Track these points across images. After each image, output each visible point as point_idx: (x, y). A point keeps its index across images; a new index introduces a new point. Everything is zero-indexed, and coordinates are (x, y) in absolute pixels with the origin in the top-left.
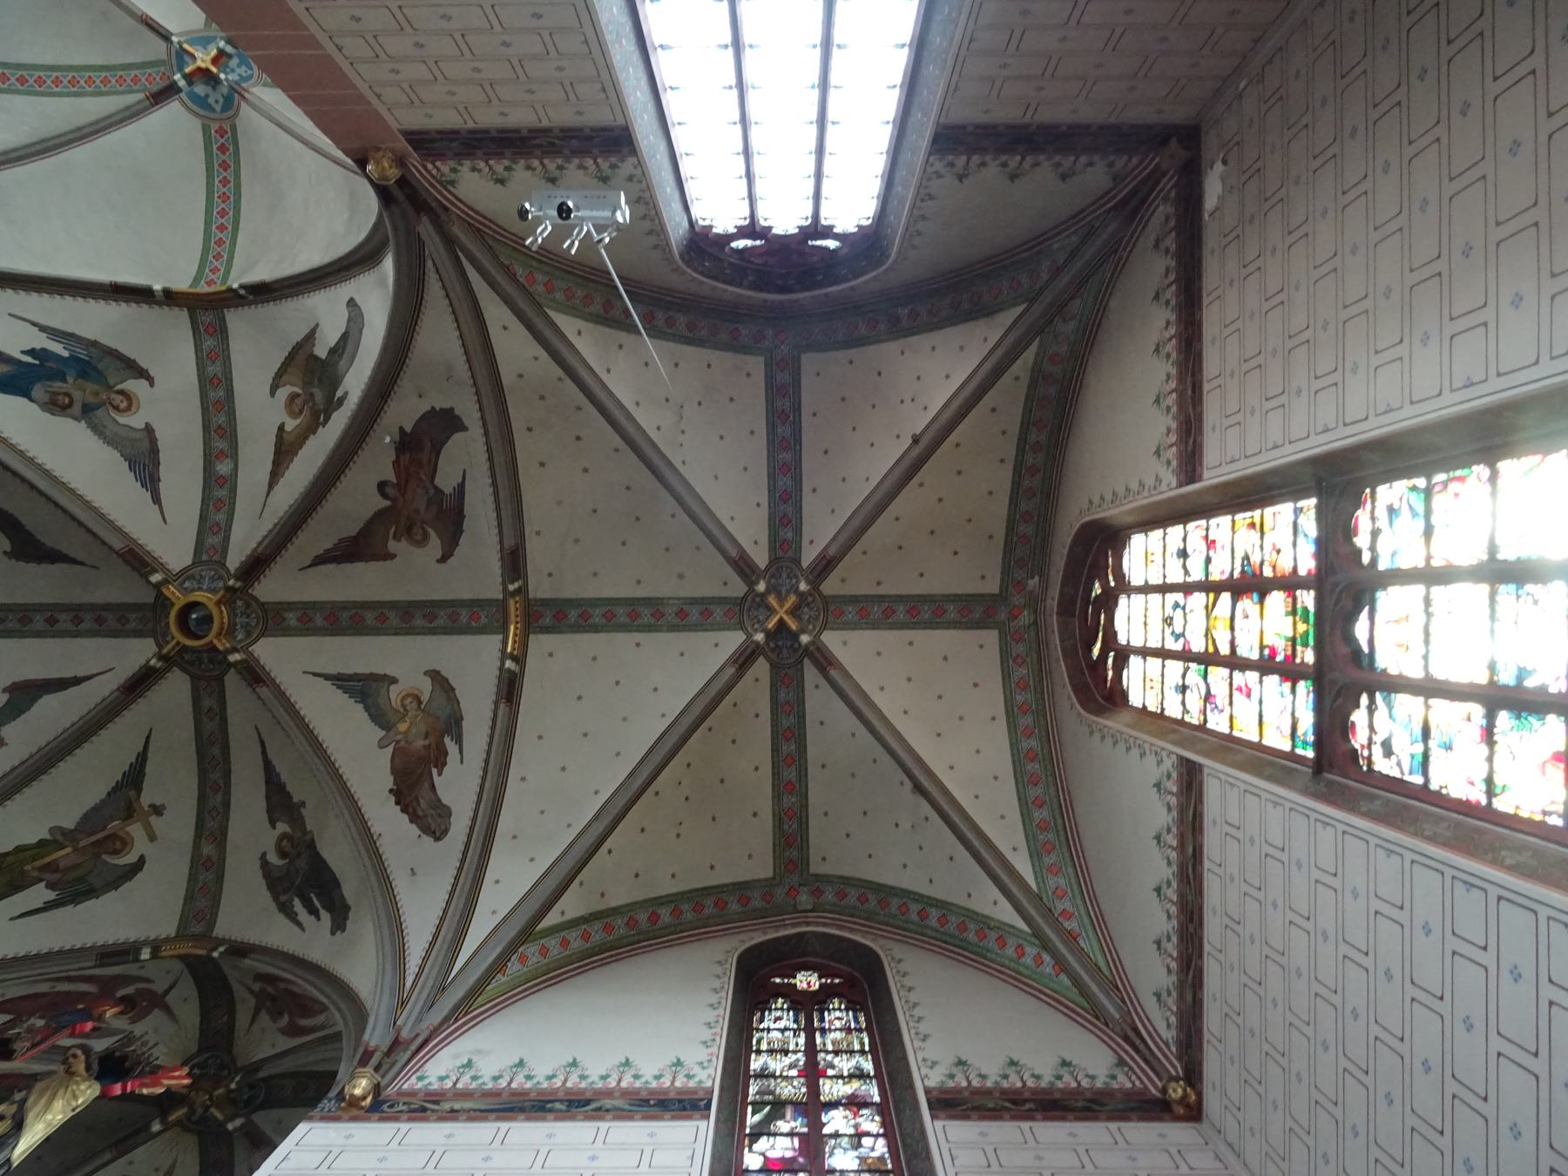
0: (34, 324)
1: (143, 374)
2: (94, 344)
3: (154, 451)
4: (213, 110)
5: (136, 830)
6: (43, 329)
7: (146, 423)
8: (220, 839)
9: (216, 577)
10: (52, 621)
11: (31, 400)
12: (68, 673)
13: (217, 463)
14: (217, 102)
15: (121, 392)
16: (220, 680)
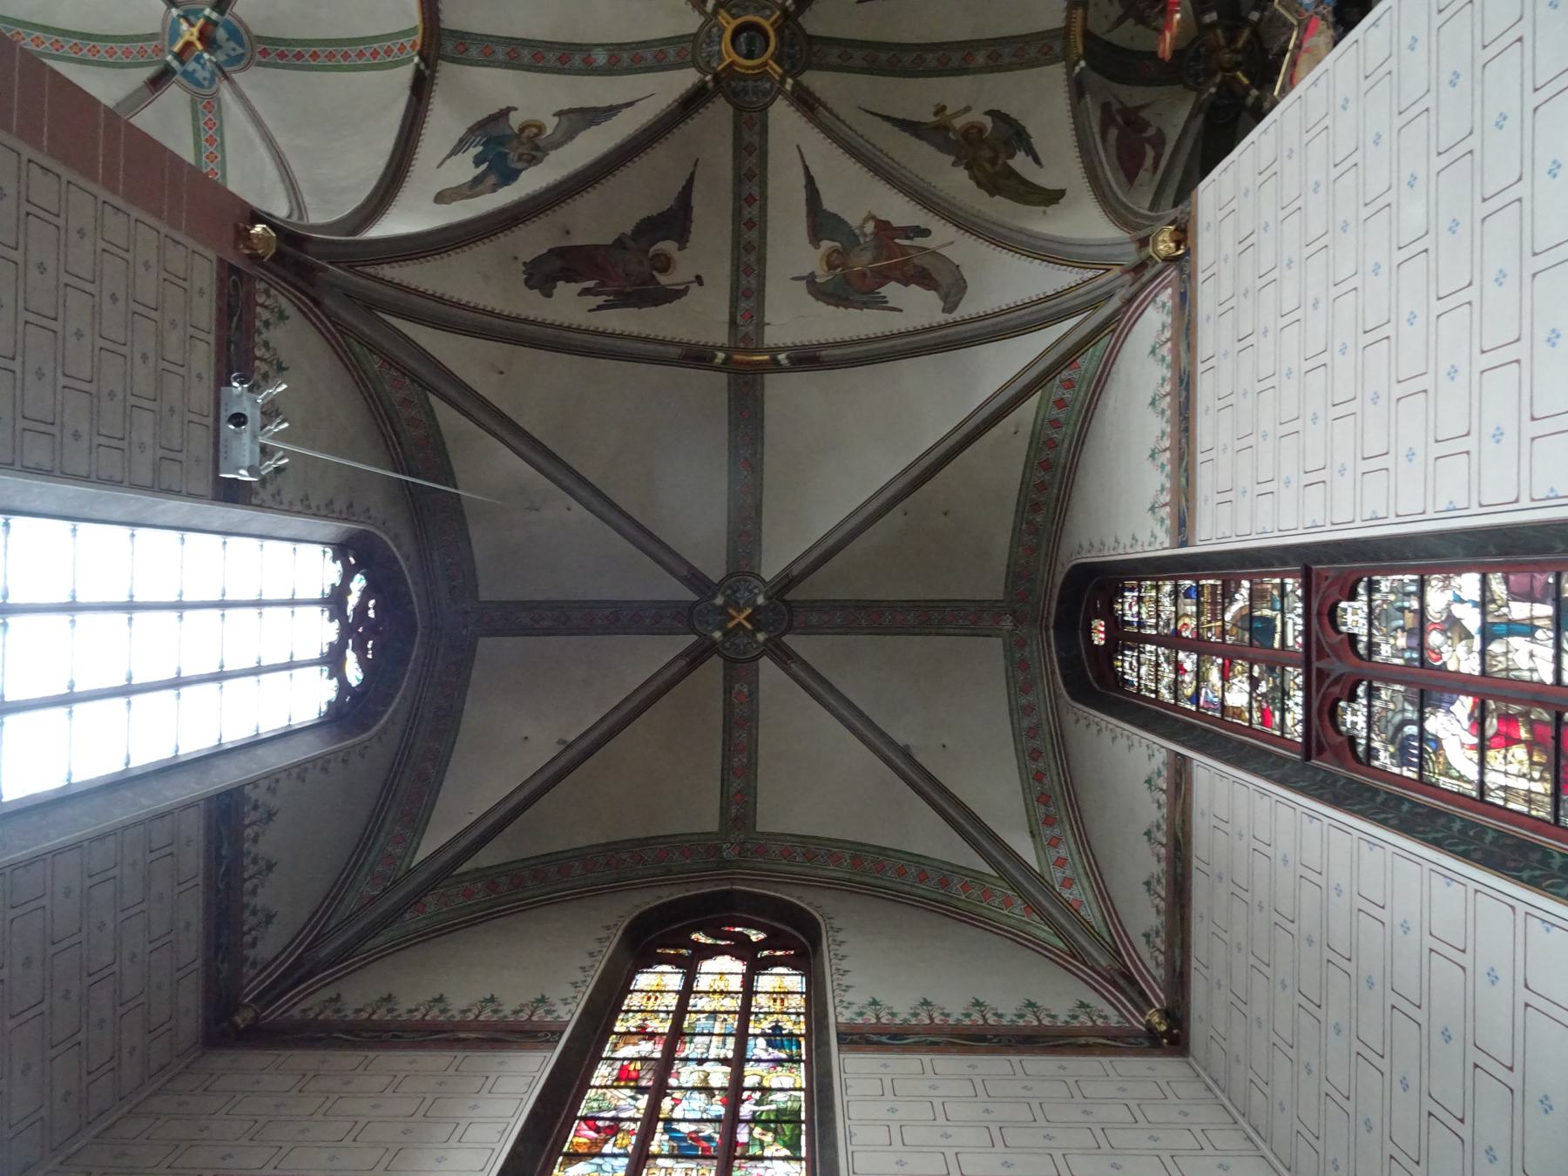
0: (449, 156)
1: (504, 113)
2: (471, 130)
3: (582, 111)
4: (243, 55)
5: (959, 123)
6: (454, 152)
7: (555, 115)
8: (968, 47)
9: (707, 40)
10: (750, 224)
11: (526, 169)
12: (802, 195)
13: (595, 65)
14: (234, 49)
15: (522, 130)
16: (812, 39)
